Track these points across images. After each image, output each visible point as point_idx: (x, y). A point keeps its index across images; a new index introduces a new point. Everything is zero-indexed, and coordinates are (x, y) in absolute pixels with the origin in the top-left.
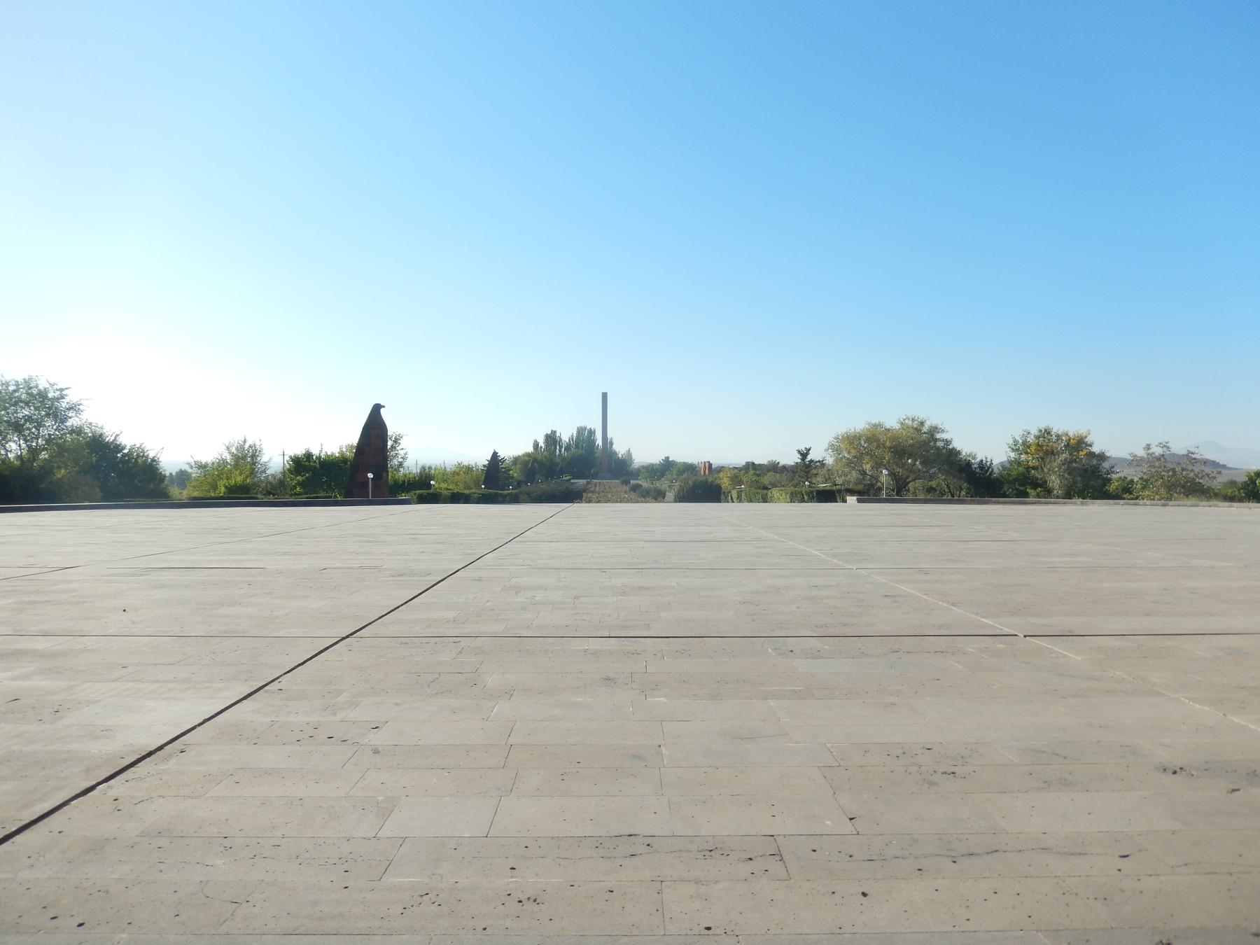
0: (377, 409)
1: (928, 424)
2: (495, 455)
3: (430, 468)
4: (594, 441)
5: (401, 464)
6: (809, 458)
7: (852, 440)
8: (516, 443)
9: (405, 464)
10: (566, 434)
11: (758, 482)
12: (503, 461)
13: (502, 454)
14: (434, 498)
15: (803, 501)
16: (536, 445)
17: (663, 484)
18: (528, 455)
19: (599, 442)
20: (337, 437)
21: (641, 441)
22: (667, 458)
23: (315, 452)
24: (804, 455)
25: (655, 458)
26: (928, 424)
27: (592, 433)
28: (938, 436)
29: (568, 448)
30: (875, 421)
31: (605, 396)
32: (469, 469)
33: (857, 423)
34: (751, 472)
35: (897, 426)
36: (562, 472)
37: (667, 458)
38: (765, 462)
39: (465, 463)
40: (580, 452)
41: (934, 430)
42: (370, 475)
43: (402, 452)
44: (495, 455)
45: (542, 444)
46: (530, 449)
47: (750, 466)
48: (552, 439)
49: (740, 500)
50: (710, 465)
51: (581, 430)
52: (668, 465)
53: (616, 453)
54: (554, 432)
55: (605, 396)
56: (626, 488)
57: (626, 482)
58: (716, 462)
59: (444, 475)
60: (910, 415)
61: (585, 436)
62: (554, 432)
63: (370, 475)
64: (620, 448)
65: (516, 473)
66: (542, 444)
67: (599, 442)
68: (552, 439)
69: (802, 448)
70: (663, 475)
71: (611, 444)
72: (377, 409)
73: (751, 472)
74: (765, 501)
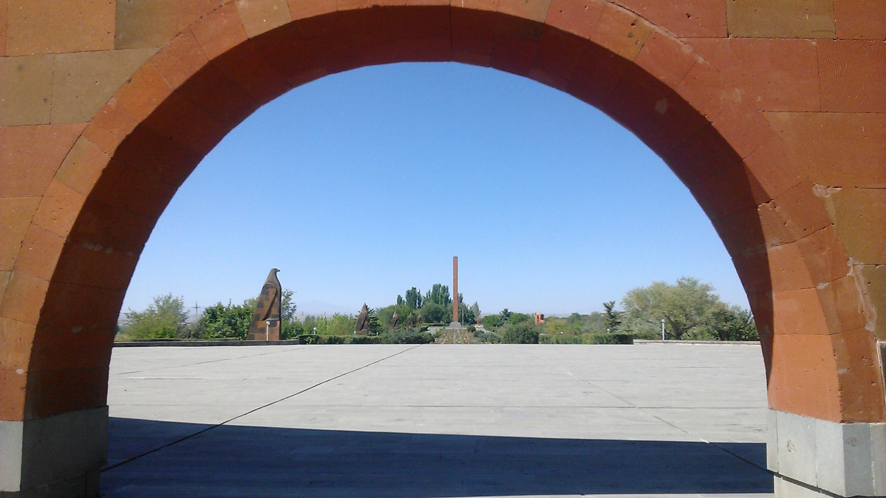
0: (275, 271)
1: (700, 283)
3: (313, 317)
5: (290, 315)
6: (613, 310)
7: (640, 296)
8: (383, 298)
9: (294, 315)
10: (424, 290)
11: (573, 330)
13: (370, 307)
14: (317, 341)
16: (400, 300)
17: (501, 331)
18: (392, 307)
19: (451, 297)
20: (241, 291)
21: (486, 296)
22: (506, 310)
23: (225, 304)
24: (609, 308)
26: (700, 283)
27: (445, 289)
28: (708, 293)
29: (427, 299)
30: (658, 280)
31: (455, 259)
33: (645, 283)
35: (676, 284)
37: (506, 310)
38: (589, 313)
39: (342, 314)
41: (707, 288)
43: (292, 306)
44: (366, 307)
45: (404, 299)
47: (576, 317)
48: (413, 295)
51: (436, 288)
52: (507, 314)
53: (465, 307)
55: (455, 259)
56: (471, 334)
59: (325, 322)
60: (686, 277)
61: (439, 293)
64: (469, 302)
66: (404, 299)
68: (413, 295)
69: (608, 302)
72: (275, 271)
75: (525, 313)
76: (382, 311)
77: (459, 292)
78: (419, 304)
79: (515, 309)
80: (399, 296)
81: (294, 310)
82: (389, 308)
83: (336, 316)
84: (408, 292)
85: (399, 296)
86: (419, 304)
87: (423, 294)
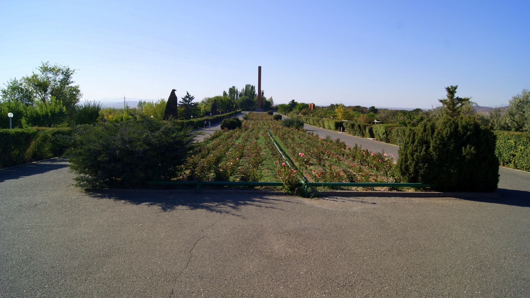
0: (174, 91)
4: (254, 92)
10: (240, 88)
16: (225, 94)
19: (257, 92)
22: (293, 101)
25: (287, 102)
27: (253, 88)
29: (241, 95)
31: (260, 68)
36: (237, 107)
40: (247, 97)
45: (228, 93)
46: (221, 95)
48: (233, 91)
50: (314, 105)
51: (247, 86)
52: (293, 104)
53: (265, 98)
55: (260, 68)
61: (249, 90)
64: (267, 96)
66: (228, 93)
67: (257, 92)
68: (233, 91)
71: (263, 93)
72: (174, 91)
77: (262, 89)
78: (237, 96)
79: (299, 100)
80: (224, 92)
85: (224, 92)
86: (237, 96)
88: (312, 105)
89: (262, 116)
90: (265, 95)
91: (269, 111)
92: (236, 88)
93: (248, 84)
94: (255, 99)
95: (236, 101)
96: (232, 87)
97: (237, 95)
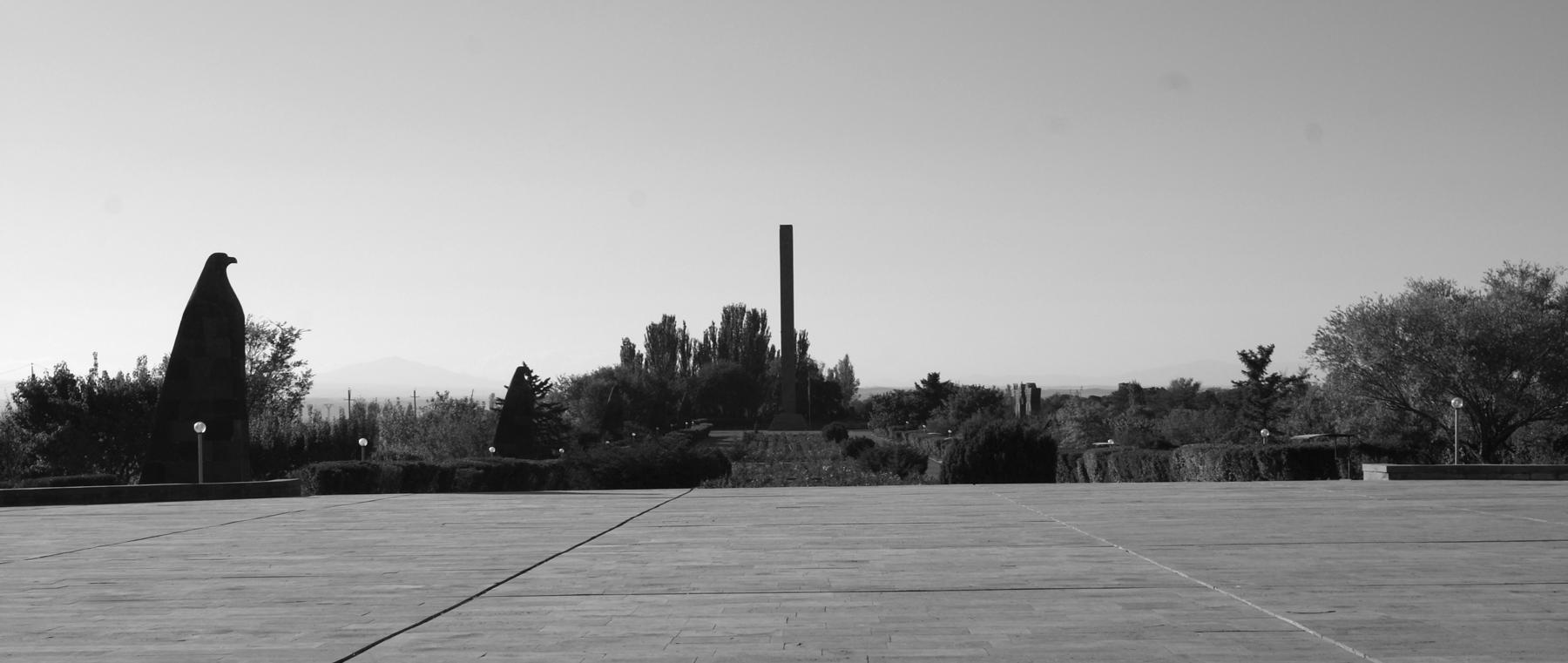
2: (523, 371)
4: (764, 340)
5: (296, 400)
8: (577, 347)
9: (309, 398)
10: (699, 323)
12: (545, 387)
15: (1254, 475)
16: (628, 350)
18: (606, 374)
19: (775, 341)
21: (873, 338)
25: (905, 377)
27: (758, 320)
29: (704, 353)
31: (786, 233)
32: (465, 409)
34: (1133, 408)
39: (457, 394)
40: (732, 365)
42: (200, 427)
43: (298, 372)
45: (641, 348)
46: (614, 360)
47: (1130, 394)
48: (664, 335)
49: (1104, 478)
50: (1036, 391)
51: (732, 315)
52: (935, 390)
53: (813, 368)
54: (669, 321)
55: (786, 233)
56: (836, 448)
57: (838, 435)
58: (1050, 383)
59: (406, 422)
61: (741, 328)
62: (669, 321)
63: (200, 427)
64: (824, 356)
65: (574, 417)
66: (641, 348)
67: (775, 341)
68: (664, 335)
70: (923, 417)
71: (804, 345)
73: (1133, 408)
74: (1163, 476)
75: (988, 385)
76: (579, 386)
77: (799, 326)
78: (684, 363)
79: (961, 372)
81: (305, 385)
82: (597, 375)
83: (443, 403)
84: (654, 331)
87: (696, 334)
88: (1028, 391)
89: (799, 448)
90: (813, 353)
91: (829, 427)
92: (679, 325)
93: (735, 301)
94: (772, 370)
95: (679, 385)
96: (658, 321)
97: (686, 355)
